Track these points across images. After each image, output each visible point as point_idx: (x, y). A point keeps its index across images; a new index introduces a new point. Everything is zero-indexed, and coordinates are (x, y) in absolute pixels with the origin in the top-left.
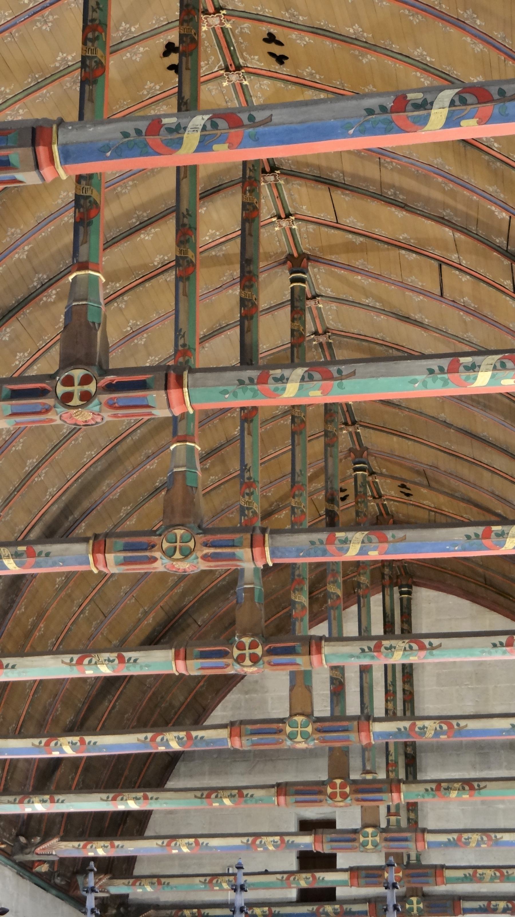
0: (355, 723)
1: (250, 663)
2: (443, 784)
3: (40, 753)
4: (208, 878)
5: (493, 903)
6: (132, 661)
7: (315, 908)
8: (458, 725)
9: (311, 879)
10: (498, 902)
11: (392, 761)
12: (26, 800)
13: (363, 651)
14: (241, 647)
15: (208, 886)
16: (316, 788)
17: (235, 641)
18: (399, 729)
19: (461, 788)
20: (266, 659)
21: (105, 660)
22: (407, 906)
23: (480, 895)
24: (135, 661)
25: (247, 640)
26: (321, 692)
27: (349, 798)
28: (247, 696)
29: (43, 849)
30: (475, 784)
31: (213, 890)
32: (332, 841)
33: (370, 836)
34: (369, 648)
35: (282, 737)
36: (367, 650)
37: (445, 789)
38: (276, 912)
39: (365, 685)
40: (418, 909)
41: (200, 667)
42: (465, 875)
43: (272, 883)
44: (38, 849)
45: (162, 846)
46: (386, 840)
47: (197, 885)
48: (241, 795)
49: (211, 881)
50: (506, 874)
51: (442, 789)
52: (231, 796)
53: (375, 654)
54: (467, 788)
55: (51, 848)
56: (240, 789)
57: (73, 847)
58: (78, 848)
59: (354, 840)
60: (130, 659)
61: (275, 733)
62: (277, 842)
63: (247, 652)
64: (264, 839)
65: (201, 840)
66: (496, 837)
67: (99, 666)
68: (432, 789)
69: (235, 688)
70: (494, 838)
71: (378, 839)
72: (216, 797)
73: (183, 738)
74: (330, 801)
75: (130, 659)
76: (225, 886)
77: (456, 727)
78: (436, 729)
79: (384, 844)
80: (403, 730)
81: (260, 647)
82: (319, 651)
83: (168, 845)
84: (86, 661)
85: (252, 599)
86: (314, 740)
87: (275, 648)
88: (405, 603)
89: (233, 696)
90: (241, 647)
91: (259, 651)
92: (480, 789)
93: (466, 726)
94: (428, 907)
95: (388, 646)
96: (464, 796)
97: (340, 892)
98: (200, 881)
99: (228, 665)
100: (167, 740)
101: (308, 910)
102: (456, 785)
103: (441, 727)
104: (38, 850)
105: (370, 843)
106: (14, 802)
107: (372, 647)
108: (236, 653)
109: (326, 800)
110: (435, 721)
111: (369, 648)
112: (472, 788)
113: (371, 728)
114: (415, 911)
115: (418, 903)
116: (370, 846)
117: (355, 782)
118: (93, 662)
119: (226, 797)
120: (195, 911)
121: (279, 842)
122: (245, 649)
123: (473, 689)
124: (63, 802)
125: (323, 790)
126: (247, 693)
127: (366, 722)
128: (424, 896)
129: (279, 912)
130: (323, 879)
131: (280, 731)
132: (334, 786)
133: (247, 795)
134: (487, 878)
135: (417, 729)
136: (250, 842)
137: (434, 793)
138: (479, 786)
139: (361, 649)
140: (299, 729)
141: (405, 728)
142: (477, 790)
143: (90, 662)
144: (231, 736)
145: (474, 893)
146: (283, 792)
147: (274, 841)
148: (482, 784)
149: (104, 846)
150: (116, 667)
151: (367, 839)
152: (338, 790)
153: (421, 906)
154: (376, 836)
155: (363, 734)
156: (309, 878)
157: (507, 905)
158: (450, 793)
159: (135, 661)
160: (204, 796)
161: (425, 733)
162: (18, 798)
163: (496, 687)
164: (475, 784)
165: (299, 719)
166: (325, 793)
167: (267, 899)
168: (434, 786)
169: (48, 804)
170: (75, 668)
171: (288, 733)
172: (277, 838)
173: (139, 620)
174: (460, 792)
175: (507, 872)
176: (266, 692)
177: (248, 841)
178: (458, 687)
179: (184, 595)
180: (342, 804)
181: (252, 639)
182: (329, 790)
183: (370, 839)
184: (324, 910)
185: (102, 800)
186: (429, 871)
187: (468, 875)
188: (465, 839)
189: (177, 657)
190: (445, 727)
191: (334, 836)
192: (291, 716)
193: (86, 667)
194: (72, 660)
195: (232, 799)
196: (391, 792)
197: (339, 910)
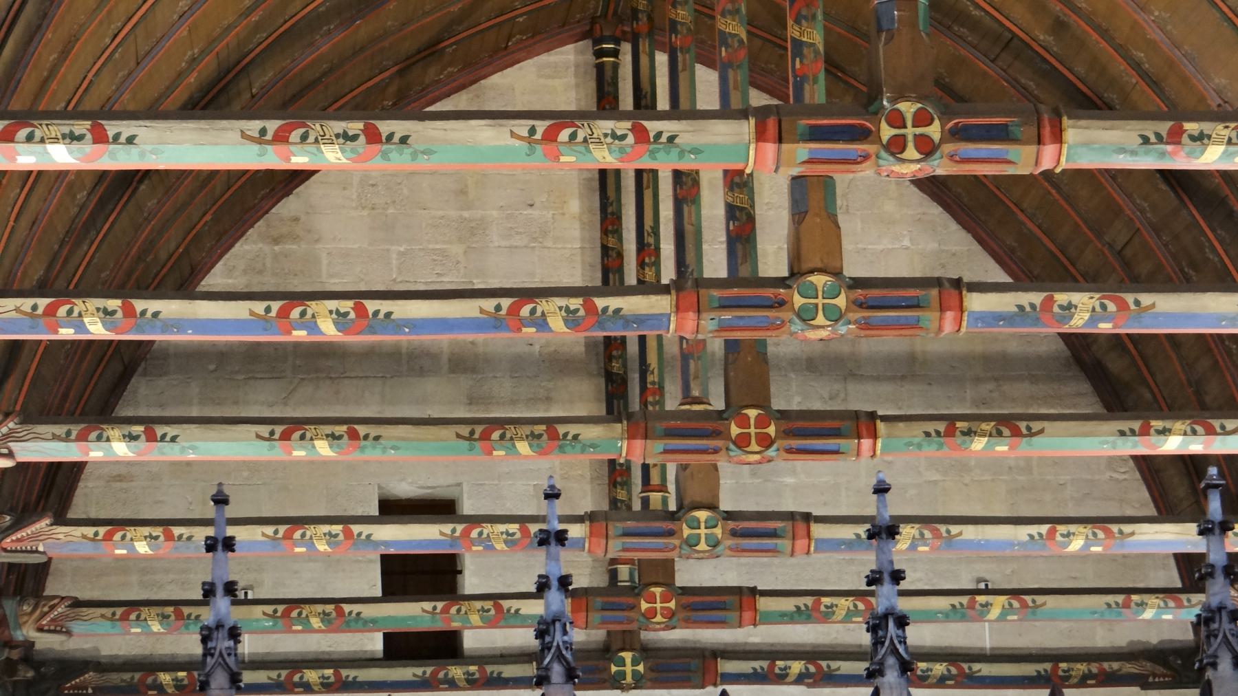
0: (934, 292)
1: (917, 156)
2: (959, 424)
3: (265, 330)
4: (281, 608)
5: (780, 664)
6: (664, 139)
7: (429, 670)
8: (1137, 303)
9: (493, 612)
10: (789, 663)
11: (653, 383)
12: (93, 435)
13: (1146, 140)
14: (897, 120)
15: (280, 623)
16: (709, 425)
17: (883, 107)
18: (1021, 308)
19: (994, 432)
20: (948, 148)
21: (606, 135)
22: (614, 669)
23: (748, 648)
24: (671, 139)
25: (908, 108)
26: (431, 246)
27: (775, 447)
28: (276, 248)
29: (18, 540)
30: (1023, 425)
31: (290, 631)
32: (626, 534)
33: (703, 525)
34: (1159, 136)
35: (784, 314)
36: (1153, 139)
37: (964, 434)
39: (688, 228)
41: (805, 158)
42: (798, 608)
43: (413, 618)
44: (8, 540)
45: (274, 539)
46: (734, 534)
47: (257, 620)
48: (554, 436)
49: (286, 614)
51: (958, 433)
52: (534, 437)
53: (1169, 148)
54: (1006, 432)
55: (35, 537)
56: (550, 422)
57: (84, 537)
58: (92, 540)
59: (670, 534)
60: (659, 135)
61: (771, 307)
62: (514, 534)
63: (910, 131)
64: (487, 529)
65: (356, 529)
66: (948, 532)
67: (591, 146)
68: (938, 433)
69: (251, 231)
70: (945, 535)
71: (718, 531)
72: (502, 437)
73: (577, 310)
74: (735, 452)
75: (659, 135)
76: (316, 622)
77: (1133, 307)
78: (1094, 309)
79: (730, 542)
80: (1028, 309)
81: (937, 123)
82: (1058, 138)
83: (288, 536)
84: (564, 135)
85: (914, 25)
86: (850, 323)
87: (966, 128)
88: (608, 73)
89: (247, 247)
90: (897, 120)
91: (934, 131)
92: (1031, 434)
93: (1153, 305)
94: (652, 670)
95: (1196, 133)
96: (998, 448)
97: (472, 640)
98: (264, 614)
99: (866, 157)
100: (543, 313)
101: (415, 675)
102: (986, 427)
103: (1104, 307)
104: (8, 542)
105: (703, 540)
106: (67, 438)
107: (1164, 134)
108: (887, 132)
109: (728, 449)
110: (1092, 294)
111: (1158, 135)
112: (1016, 433)
113: (965, 304)
115: (635, 662)
116: (703, 546)
117: (783, 415)
118: (580, 138)
119: (521, 439)
120: (182, 674)
121: (518, 535)
122: (905, 127)
124: (173, 439)
125: (722, 429)
126: (276, 241)
127: (954, 292)
128: (646, 652)
129: (355, 678)
130: (517, 611)
131: (781, 304)
132: (744, 422)
133: (566, 435)
134: (840, 614)
135: (1056, 309)
136: (457, 534)
137: (942, 440)
138: (1029, 429)
139: (1141, 136)
140: (820, 301)
141: (1033, 306)
142: (1026, 436)
143: (573, 136)
144: (678, 308)
145: (736, 644)
146: (642, 431)
147: (508, 534)
148: (1036, 426)
149: (151, 537)
150: (629, 150)
151: (697, 531)
152: (752, 430)
153: (641, 668)
154: (715, 526)
155: (949, 315)
156: (488, 610)
157: (807, 669)
158: (972, 442)
159: (671, 139)
160: (476, 436)
161: (1071, 317)
162: (75, 430)
164: (1023, 425)
165: (819, 280)
166: (728, 437)
167: (323, 653)
168: (941, 426)
169: (142, 444)
170: (539, 148)
171: (796, 307)
172: (513, 528)
173: (180, 75)
174: (993, 440)
176: (317, 241)
177: (454, 531)
179: (257, 27)
180: (757, 457)
181: (920, 105)
182: (735, 430)
183: (703, 531)
184: (446, 675)
185: (259, 437)
186: (727, 599)
187: (803, 608)
189: (760, 136)
190: (1112, 307)
191: (630, 524)
192: (796, 272)
193: (561, 148)
194: (532, 131)
195: (535, 442)
196: (859, 437)
197: (477, 676)
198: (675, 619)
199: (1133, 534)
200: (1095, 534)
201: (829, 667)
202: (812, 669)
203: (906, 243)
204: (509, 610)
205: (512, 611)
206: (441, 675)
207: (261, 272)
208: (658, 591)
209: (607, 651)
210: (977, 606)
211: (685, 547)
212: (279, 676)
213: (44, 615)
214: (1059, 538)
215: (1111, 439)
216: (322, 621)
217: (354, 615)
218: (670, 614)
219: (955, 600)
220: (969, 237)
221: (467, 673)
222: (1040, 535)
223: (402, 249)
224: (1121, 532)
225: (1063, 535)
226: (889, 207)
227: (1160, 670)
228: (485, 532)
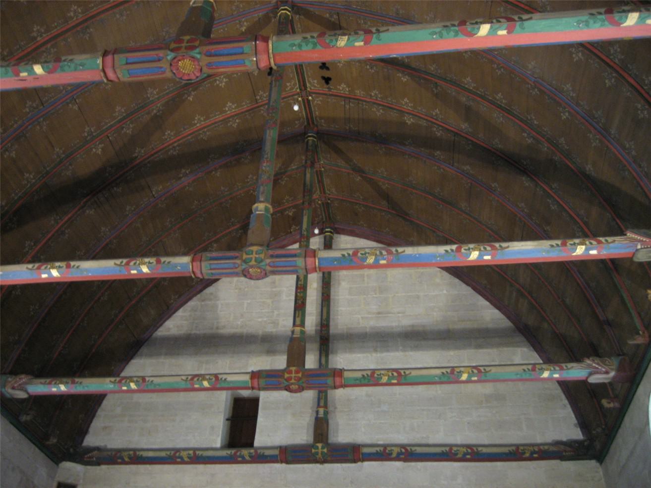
9: (214, 379)
10: (393, 448)
11: (301, 285)
28: (203, 303)
38: (200, 455)
40: (322, 453)
50: (403, 374)
66: (397, 251)
70: (394, 252)
96: (357, 44)
98: (110, 381)
101: (227, 454)
114: (320, 455)
115: (323, 448)
123: (376, 297)
126: (203, 301)
130: (225, 379)
157: (401, 450)
163: (395, 296)
175: (405, 373)
176: (218, 300)
178: (365, 296)
187: (366, 375)
188: (362, 254)
198: (301, 382)
199: (508, 247)
200: (485, 249)
201: (411, 449)
202: (403, 450)
203: (445, 292)
204: (221, 379)
205: (223, 379)
206: (238, 454)
207: (195, 311)
208: (293, 369)
209: (313, 446)
210: (455, 373)
211: (243, 264)
212: (170, 453)
213: (16, 382)
214: (463, 250)
215: (438, 30)
216: (136, 385)
217: (150, 382)
218: (299, 379)
219: (444, 371)
220: (470, 288)
221: (250, 453)
222: (452, 250)
223: (249, 302)
224: (500, 246)
225: (465, 250)
226: (438, 280)
227: (568, 449)
228: (138, 262)
